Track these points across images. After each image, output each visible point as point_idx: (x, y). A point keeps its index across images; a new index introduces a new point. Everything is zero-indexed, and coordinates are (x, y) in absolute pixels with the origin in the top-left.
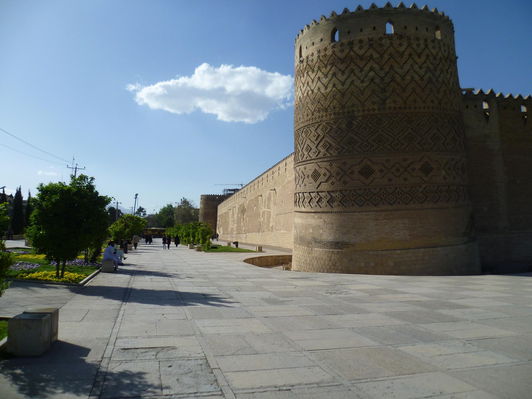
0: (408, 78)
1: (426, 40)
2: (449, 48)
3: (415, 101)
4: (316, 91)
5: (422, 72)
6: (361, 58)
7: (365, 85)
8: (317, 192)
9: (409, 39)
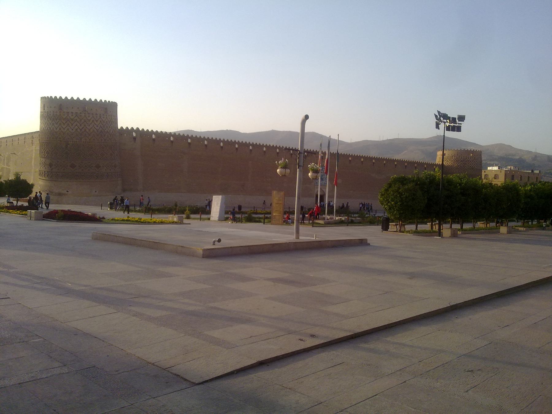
0: (91, 130)
1: (100, 115)
2: (111, 116)
3: (94, 139)
4: (52, 129)
5: (98, 128)
6: (72, 120)
7: (73, 131)
8: (51, 172)
9: (93, 114)
